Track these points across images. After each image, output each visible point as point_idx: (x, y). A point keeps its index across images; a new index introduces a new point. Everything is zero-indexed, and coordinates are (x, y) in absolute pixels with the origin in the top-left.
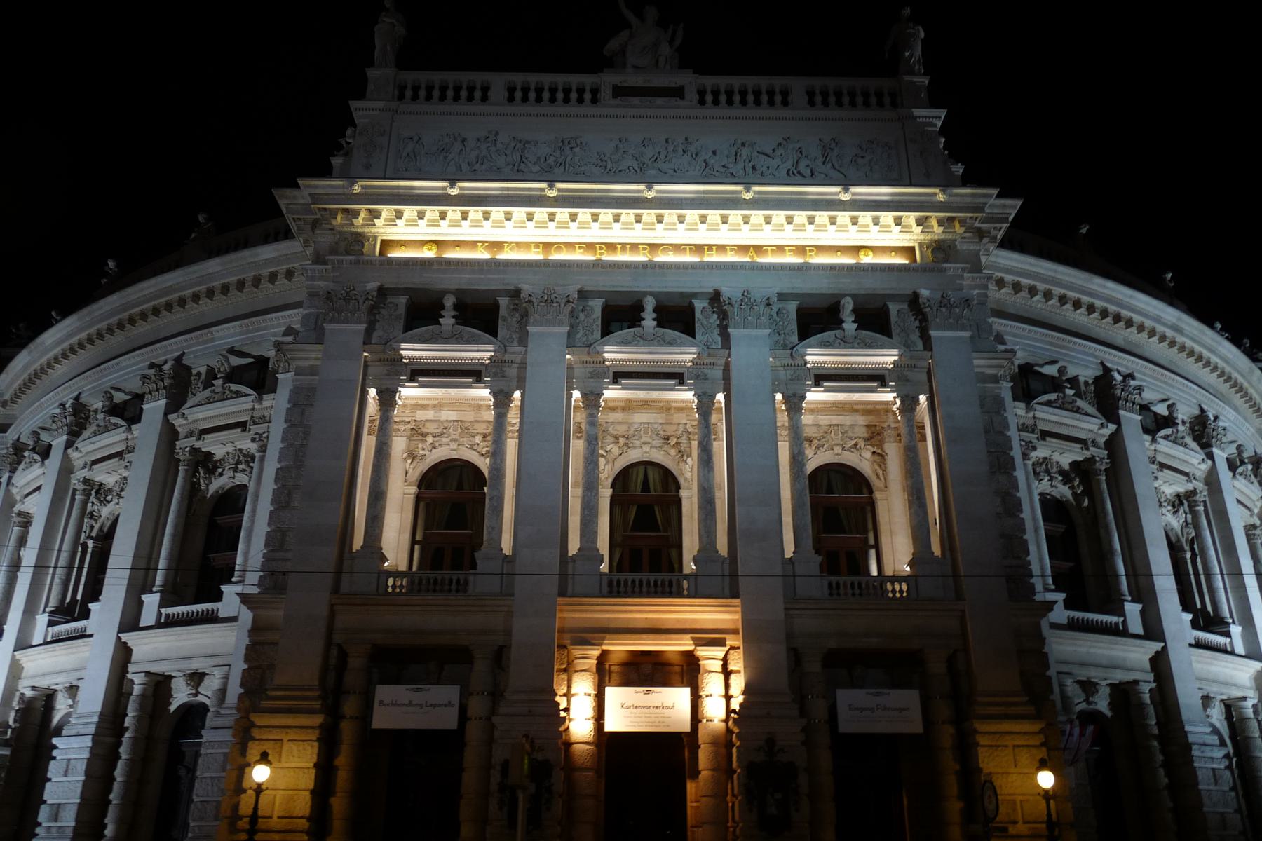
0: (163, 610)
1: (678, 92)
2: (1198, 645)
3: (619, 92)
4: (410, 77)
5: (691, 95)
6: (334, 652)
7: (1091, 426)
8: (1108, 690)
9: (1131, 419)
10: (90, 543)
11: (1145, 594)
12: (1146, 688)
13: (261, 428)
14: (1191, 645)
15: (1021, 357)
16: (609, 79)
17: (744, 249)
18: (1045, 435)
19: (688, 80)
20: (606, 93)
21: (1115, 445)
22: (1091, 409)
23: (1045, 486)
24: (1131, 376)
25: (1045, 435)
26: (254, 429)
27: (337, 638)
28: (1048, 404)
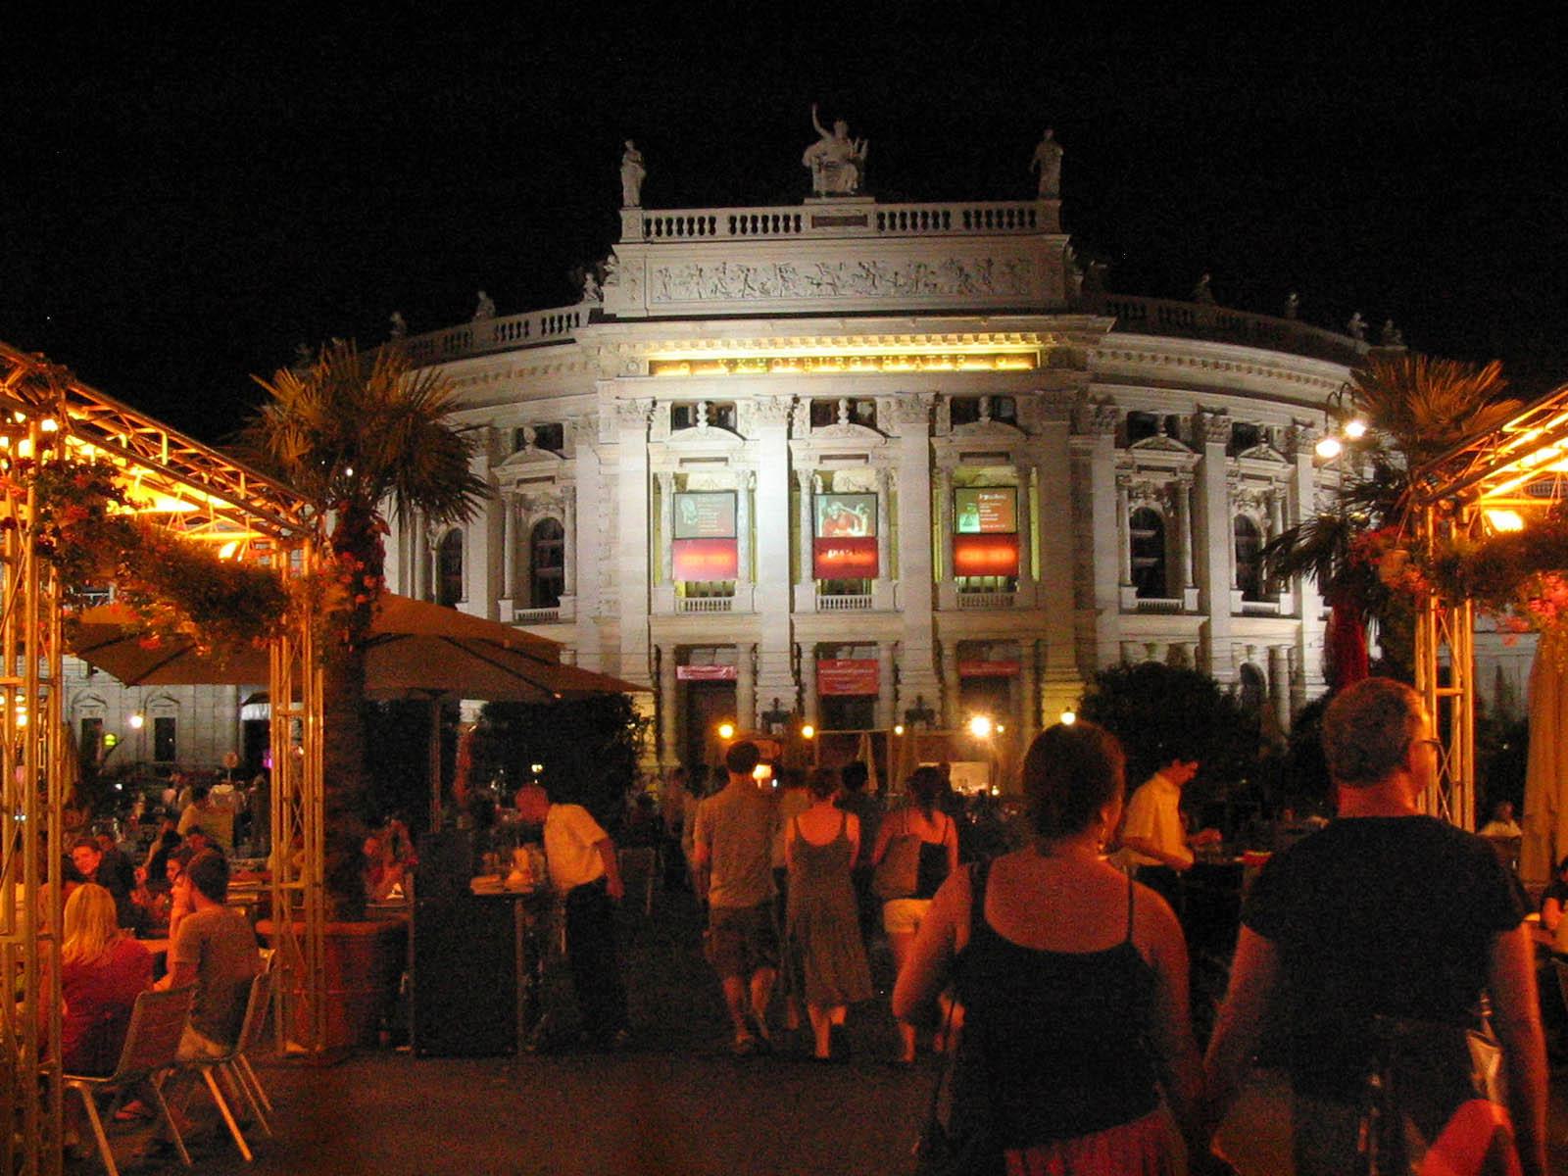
0: (518, 612)
1: (862, 221)
2: (1248, 613)
3: (817, 222)
4: (653, 215)
5: (873, 221)
6: (653, 650)
7: (1182, 458)
8: (1167, 648)
9: (1216, 449)
10: (434, 553)
11: (1201, 582)
12: (1191, 649)
13: (566, 483)
14: (1234, 615)
15: (1125, 410)
16: (807, 210)
17: (911, 358)
18: (1141, 468)
19: (868, 207)
20: (805, 224)
21: (1199, 471)
22: (1181, 446)
23: (1141, 503)
24: (1224, 412)
25: (1141, 468)
26: (560, 484)
27: (654, 641)
28: (1145, 447)
